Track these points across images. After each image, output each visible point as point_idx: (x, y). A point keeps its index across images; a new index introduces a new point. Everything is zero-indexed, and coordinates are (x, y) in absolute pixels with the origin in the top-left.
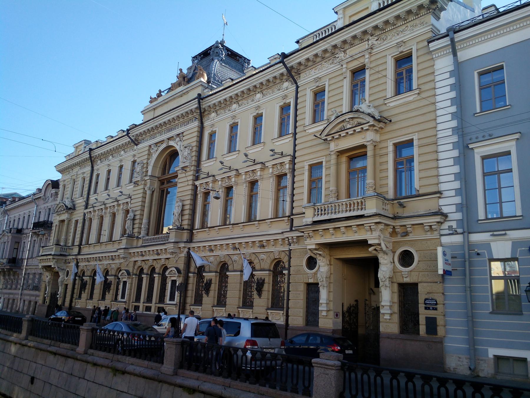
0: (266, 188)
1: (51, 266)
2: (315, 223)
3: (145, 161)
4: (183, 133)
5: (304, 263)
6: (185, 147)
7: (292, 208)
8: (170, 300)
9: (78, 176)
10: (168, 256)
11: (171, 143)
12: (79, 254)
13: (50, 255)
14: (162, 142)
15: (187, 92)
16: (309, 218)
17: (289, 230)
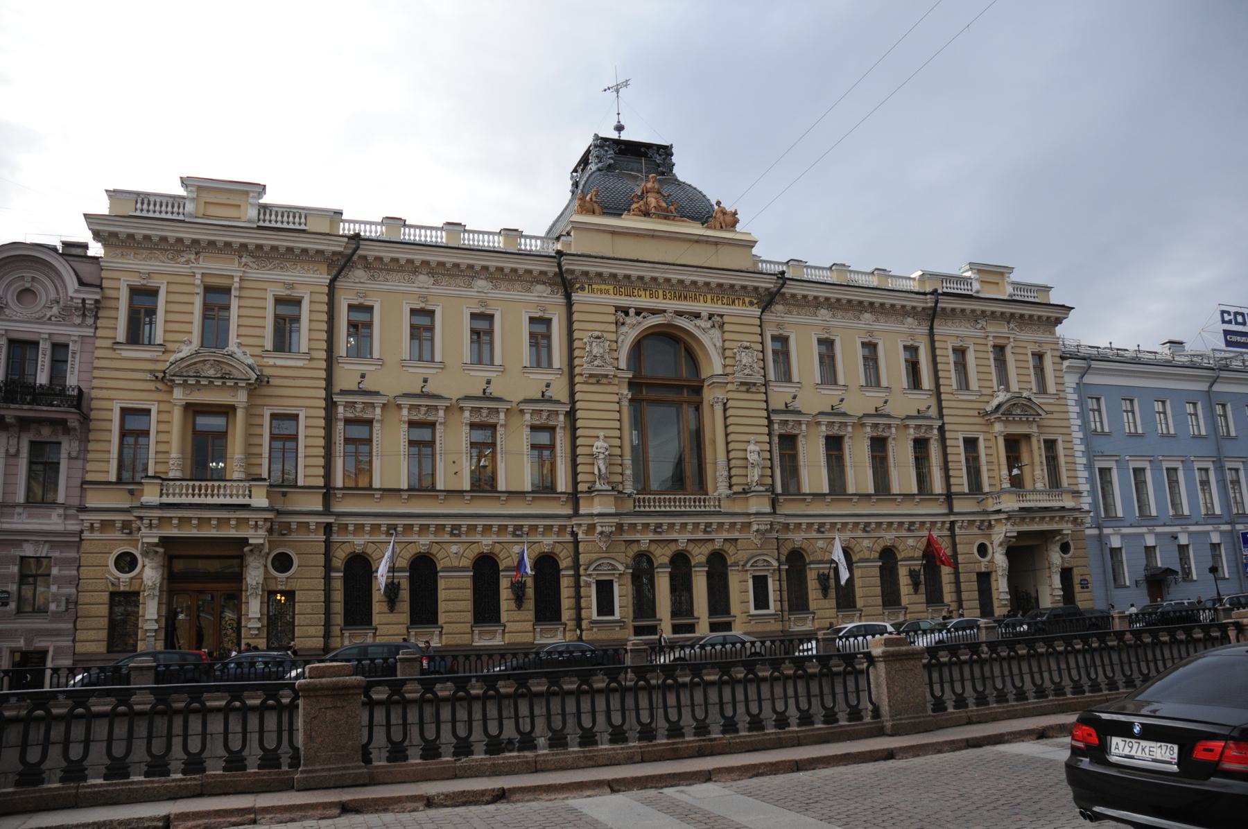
0: (901, 455)
1: (247, 539)
2: (1022, 509)
3: (613, 337)
4: (721, 316)
5: (975, 551)
6: (746, 348)
7: (948, 485)
8: (756, 608)
9: (246, 284)
10: (736, 535)
11: (682, 322)
12: (327, 511)
13: (245, 507)
14: (654, 312)
15: (716, 244)
16: (1010, 503)
17: (946, 511)
